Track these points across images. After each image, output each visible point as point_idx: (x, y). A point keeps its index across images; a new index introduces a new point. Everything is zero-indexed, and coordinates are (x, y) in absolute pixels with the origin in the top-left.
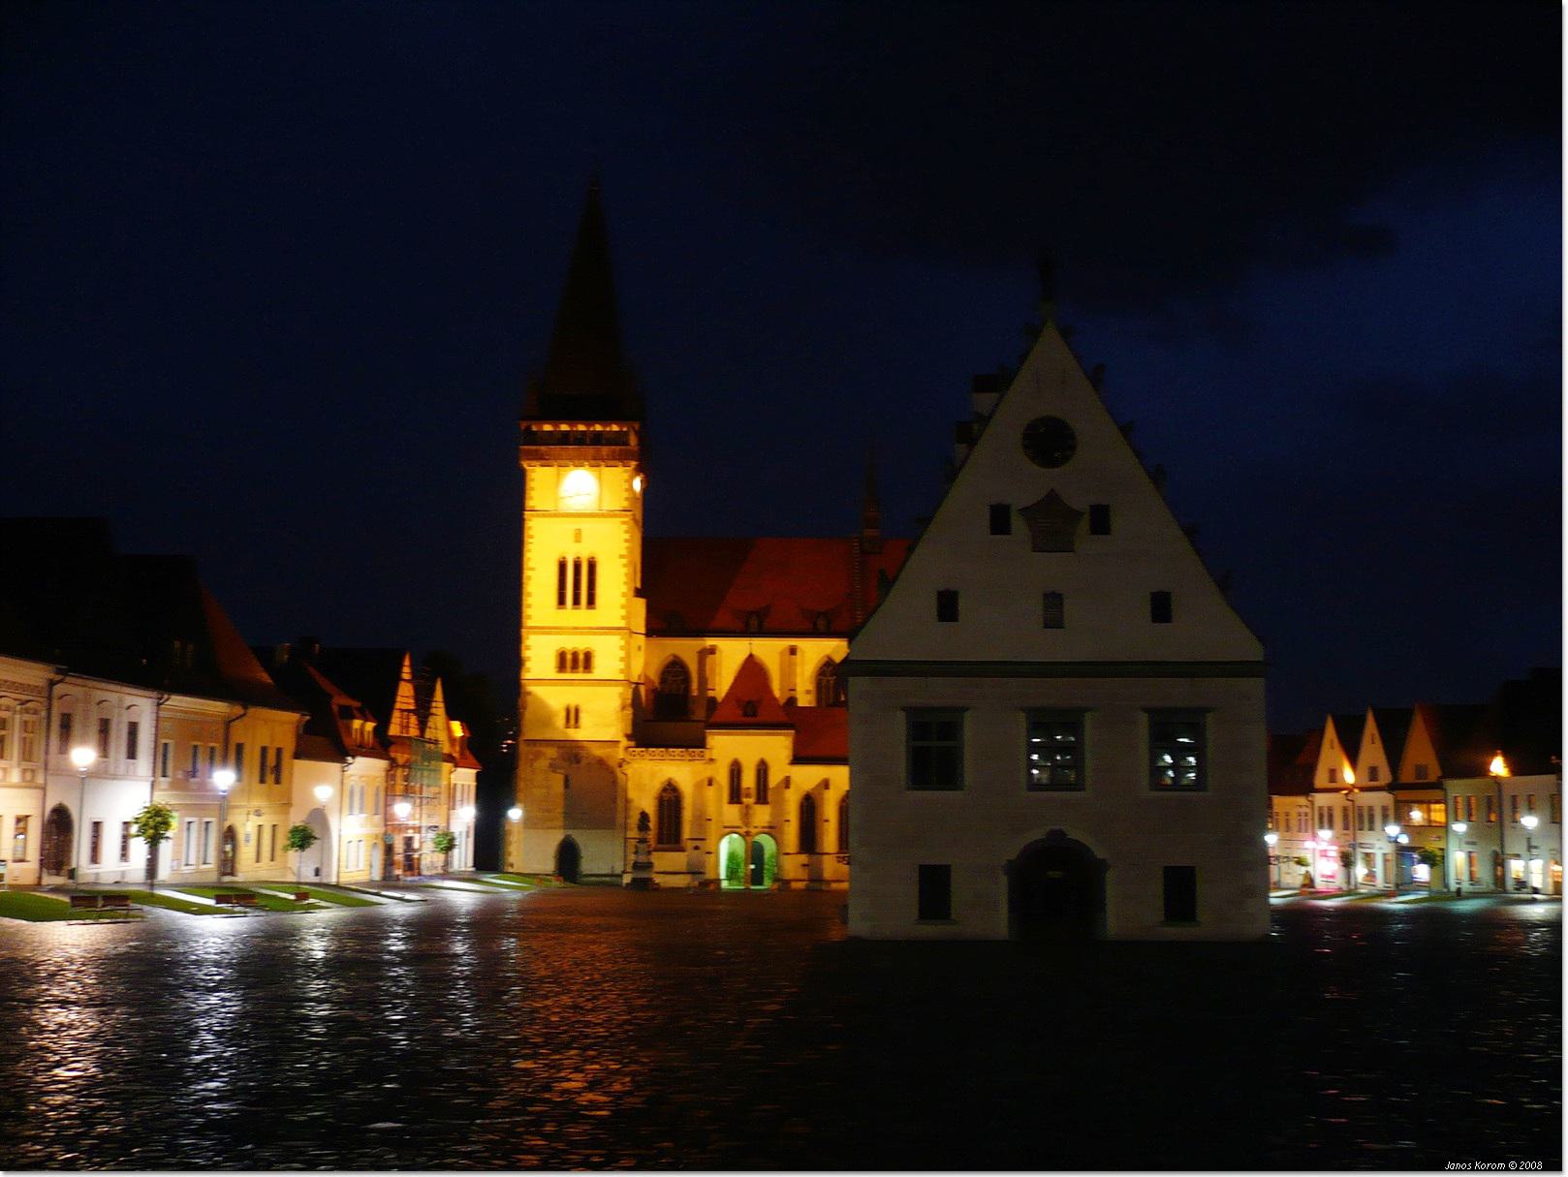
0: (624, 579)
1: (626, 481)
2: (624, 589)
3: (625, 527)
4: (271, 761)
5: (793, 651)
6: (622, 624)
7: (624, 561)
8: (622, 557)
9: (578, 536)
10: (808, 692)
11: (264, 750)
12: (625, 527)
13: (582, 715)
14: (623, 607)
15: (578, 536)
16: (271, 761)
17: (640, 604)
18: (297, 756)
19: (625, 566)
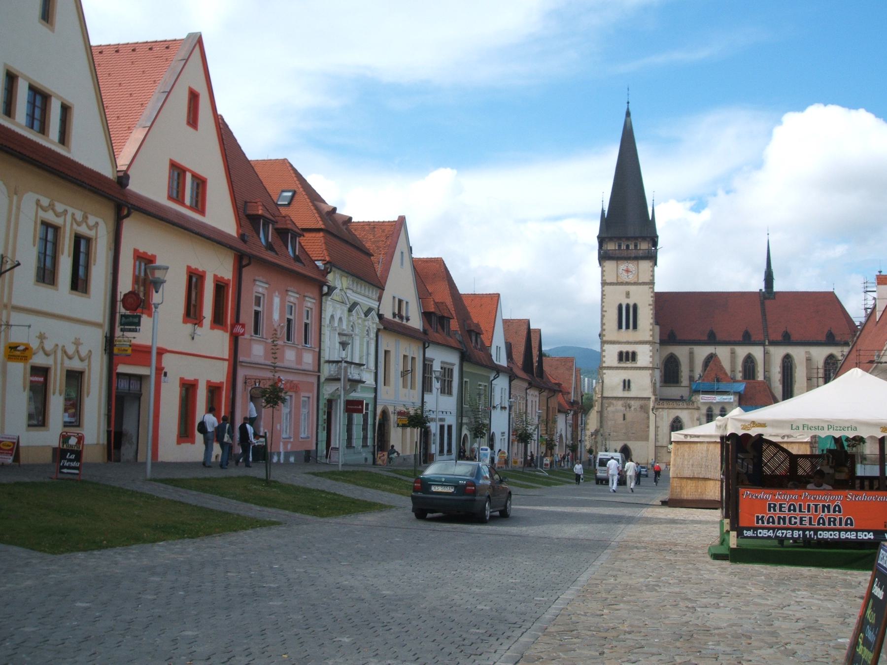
0: (651, 316)
1: (651, 267)
2: (651, 321)
3: (651, 290)
5: (733, 353)
6: (651, 339)
7: (651, 307)
8: (650, 305)
9: (628, 295)
10: (740, 372)
12: (651, 290)
13: (632, 385)
14: (651, 330)
15: (628, 295)
17: (657, 328)
19: (651, 309)
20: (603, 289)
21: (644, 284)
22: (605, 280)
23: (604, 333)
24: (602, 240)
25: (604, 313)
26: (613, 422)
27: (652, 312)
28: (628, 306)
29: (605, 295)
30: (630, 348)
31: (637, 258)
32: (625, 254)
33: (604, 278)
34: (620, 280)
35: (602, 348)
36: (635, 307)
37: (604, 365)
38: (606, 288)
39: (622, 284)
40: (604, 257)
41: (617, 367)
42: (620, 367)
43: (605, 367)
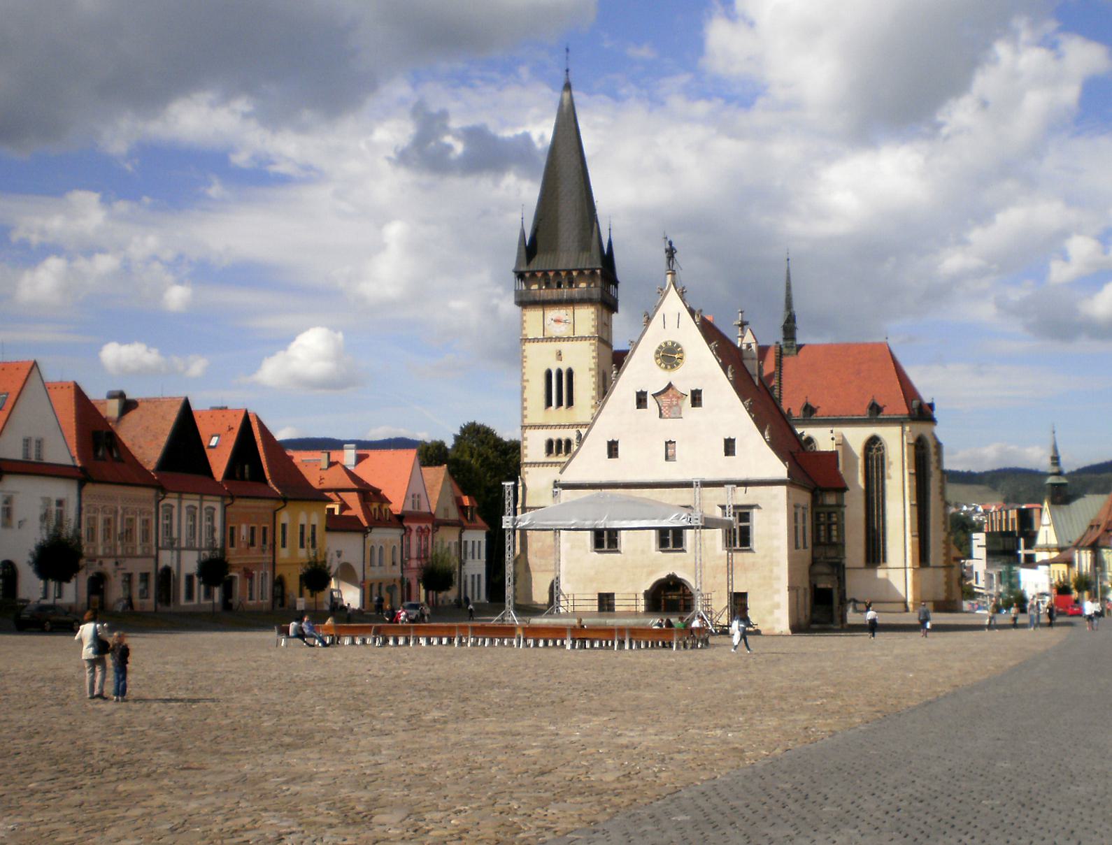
2: (594, 393)
4: (308, 533)
7: (593, 373)
8: (590, 370)
9: (559, 354)
11: (302, 526)
12: (593, 347)
16: (308, 533)
18: (328, 529)
19: (593, 376)
20: (524, 348)
21: (583, 338)
22: (526, 335)
23: (525, 413)
24: (520, 276)
25: (525, 384)
26: (540, 544)
27: (594, 379)
28: (559, 373)
29: (526, 357)
30: (563, 434)
31: (570, 302)
32: (553, 293)
33: (524, 332)
34: (547, 335)
35: (522, 435)
36: (570, 373)
37: (526, 460)
38: (528, 347)
39: (550, 339)
40: (525, 302)
41: (544, 463)
42: (548, 463)
43: (527, 463)
